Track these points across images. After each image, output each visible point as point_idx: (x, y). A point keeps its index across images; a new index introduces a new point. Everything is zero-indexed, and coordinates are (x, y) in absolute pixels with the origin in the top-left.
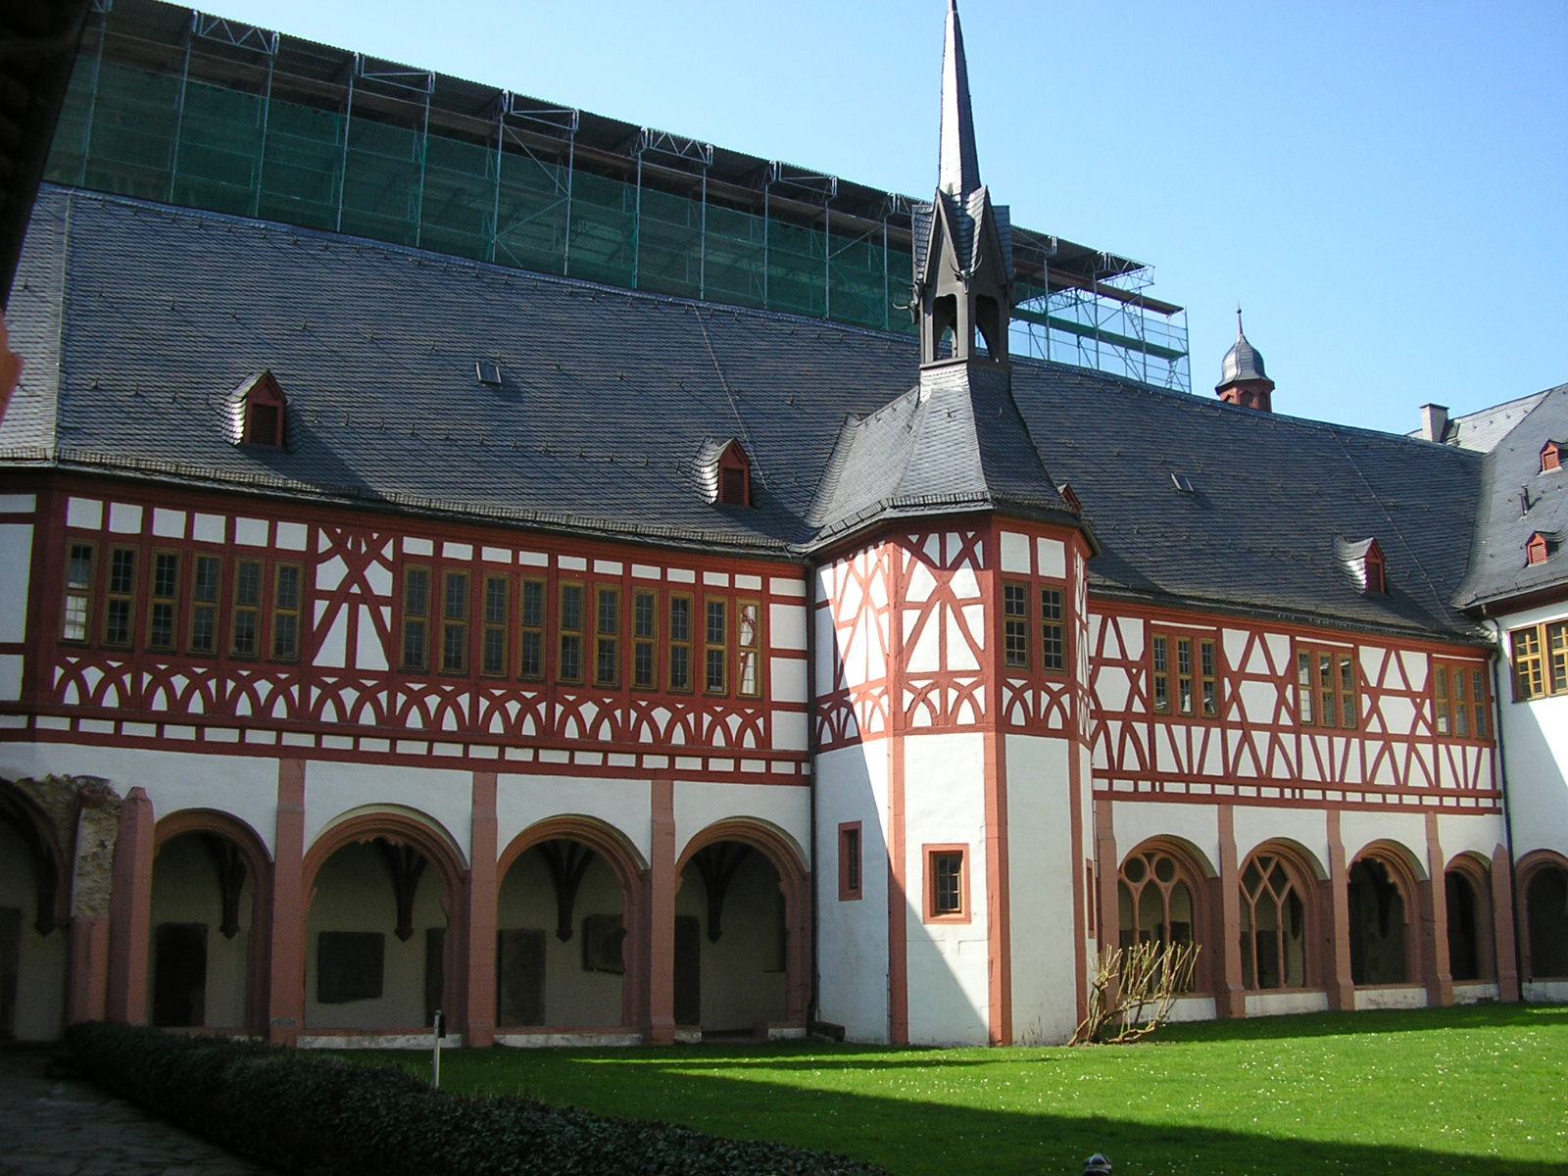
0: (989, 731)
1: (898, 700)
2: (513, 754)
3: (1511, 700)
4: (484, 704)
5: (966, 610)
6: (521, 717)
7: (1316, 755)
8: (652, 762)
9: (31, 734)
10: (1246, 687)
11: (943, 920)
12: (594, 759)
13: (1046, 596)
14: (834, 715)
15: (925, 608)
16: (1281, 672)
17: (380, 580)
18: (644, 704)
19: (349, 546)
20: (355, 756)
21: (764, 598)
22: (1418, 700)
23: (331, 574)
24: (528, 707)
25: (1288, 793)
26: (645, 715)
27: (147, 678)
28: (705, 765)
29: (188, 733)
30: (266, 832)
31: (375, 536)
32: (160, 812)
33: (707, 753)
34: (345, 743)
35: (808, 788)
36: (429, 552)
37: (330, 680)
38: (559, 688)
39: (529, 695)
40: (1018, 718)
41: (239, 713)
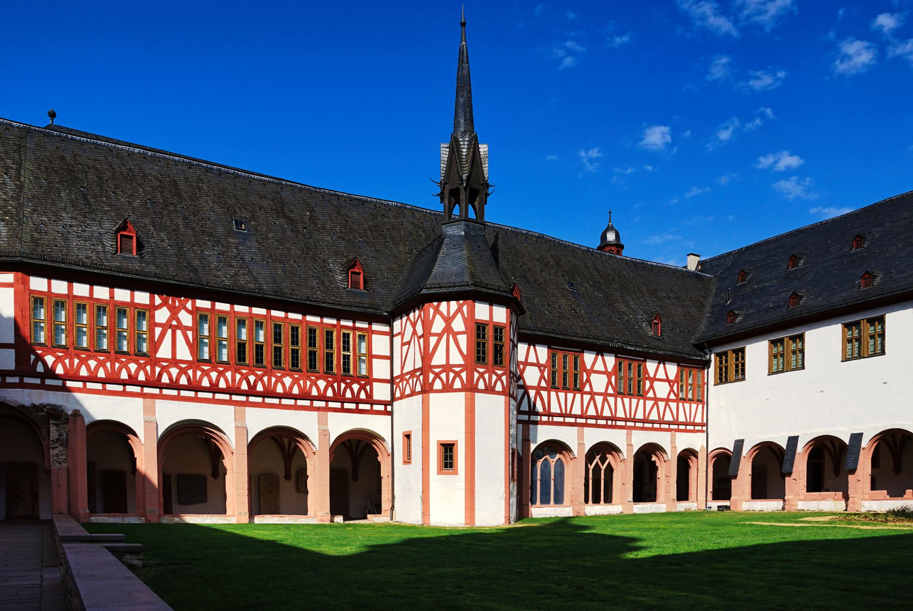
1: (426, 378)
2: (252, 399)
3: (713, 384)
5: (458, 337)
6: (256, 382)
7: (622, 407)
8: (317, 404)
9: (22, 385)
10: (593, 377)
12: (291, 402)
13: (496, 330)
14: (401, 384)
15: (440, 336)
16: (610, 369)
18: (313, 378)
22: (672, 384)
25: (610, 423)
28: (342, 405)
35: (390, 417)
36: (209, 307)
37: (165, 364)
39: (259, 373)
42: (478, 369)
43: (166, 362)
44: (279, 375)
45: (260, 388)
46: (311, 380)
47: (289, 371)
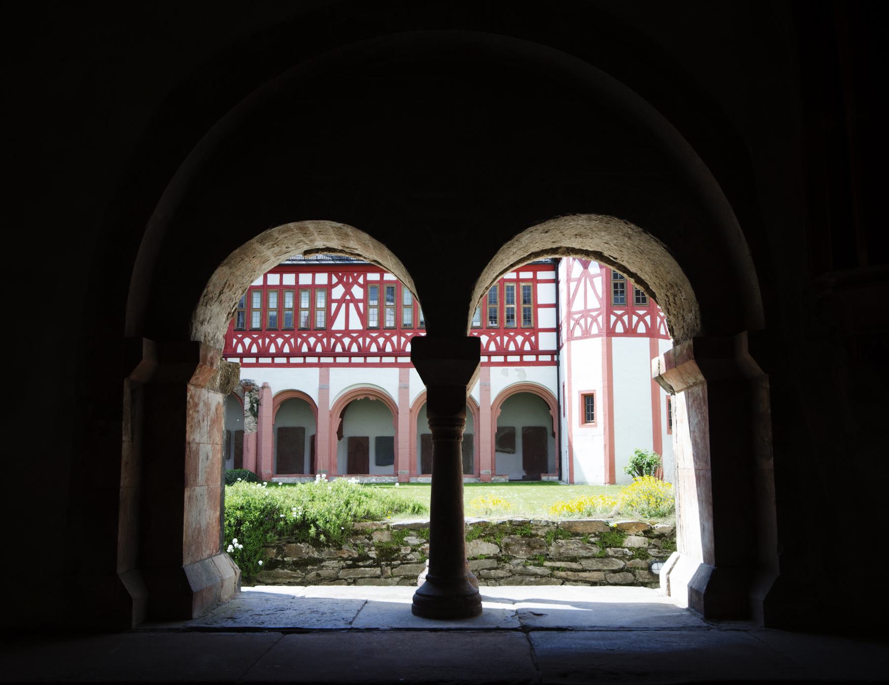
0: (603, 336)
11: (587, 426)
15: (579, 280)
17: (358, 292)
19: (345, 280)
20: (350, 365)
21: (535, 281)
23: (338, 292)
27: (267, 340)
28: (506, 359)
29: (283, 360)
31: (355, 274)
34: (346, 360)
35: (556, 367)
37: (339, 335)
42: (615, 312)
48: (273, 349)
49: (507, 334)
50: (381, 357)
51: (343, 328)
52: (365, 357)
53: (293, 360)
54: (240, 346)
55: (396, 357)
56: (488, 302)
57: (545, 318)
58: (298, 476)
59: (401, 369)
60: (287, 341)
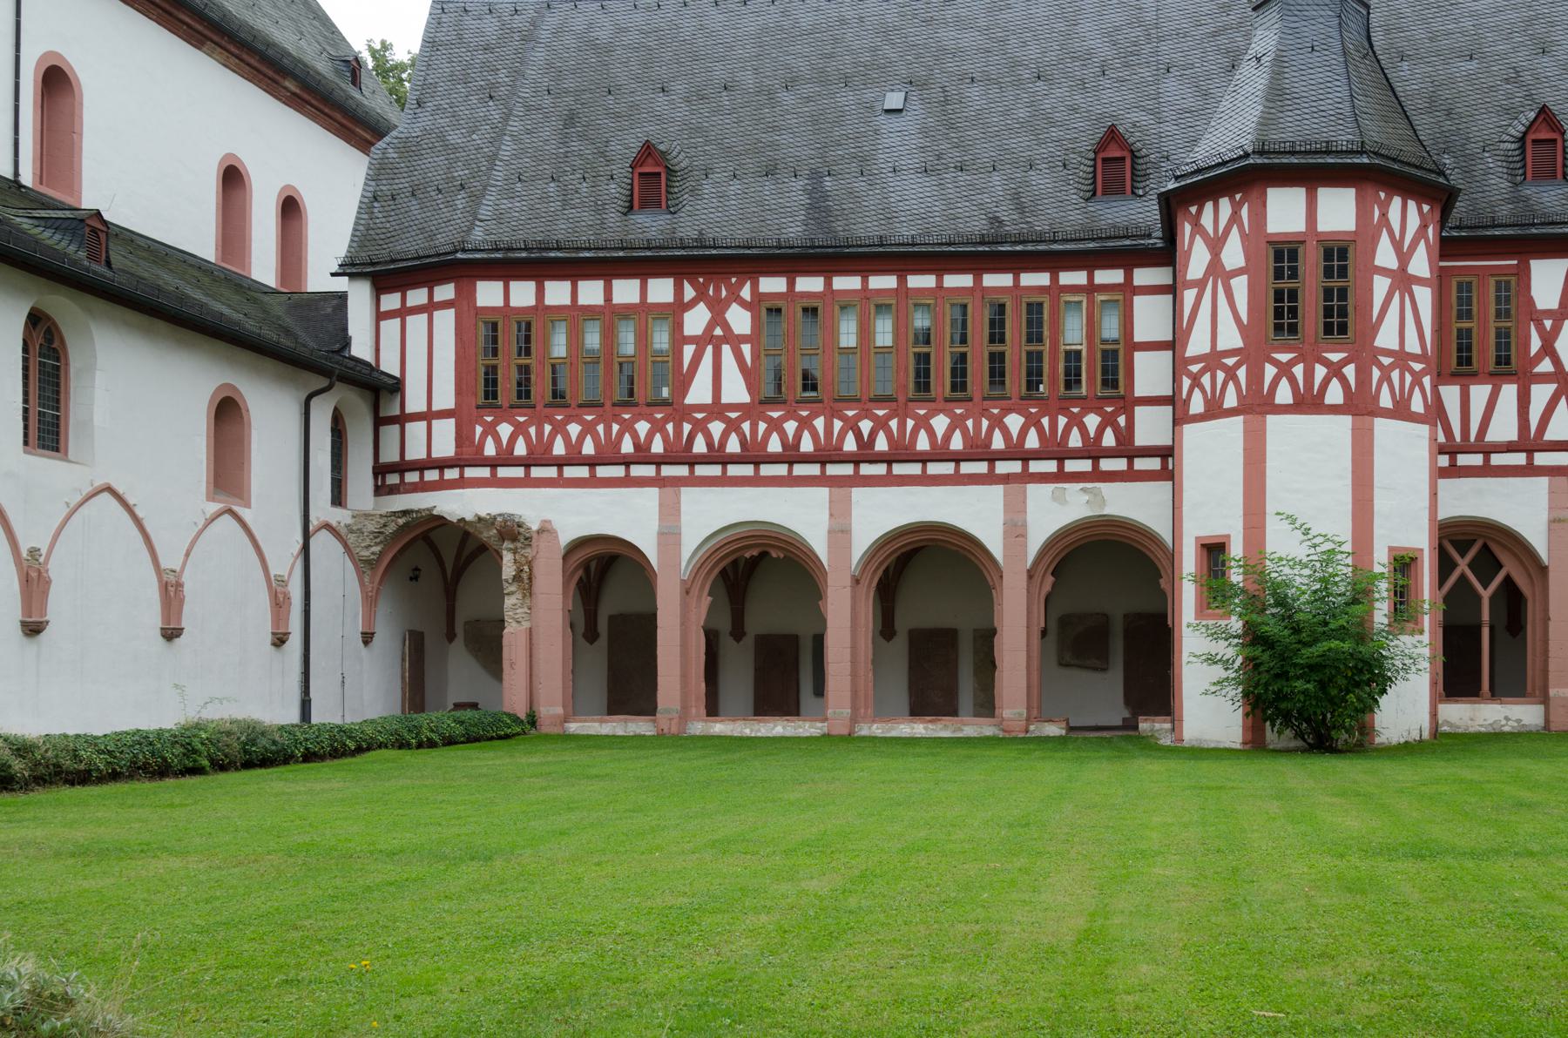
2: (866, 469)
4: (838, 424)
6: (873, 434)
8: (1002, 467)
9: (462, 483)
12: (947, 468)
17: (740, 320)
19: (711, 293)
20: (724, 481)
23: (696, 320)
24: (881, 424)
26: (998, 423)
27: (548, 428)
30: (650, 549)
31: (734, 280)
32: (566, 536)
33: (1061, 454)
34: (715, 470)
37: (699, 416)
38: (910, 404)
39: (881, 413)
40: (1386, 401)
41: (624, 450)
43: (700, 412)
44: (922, 412)
45: (881, 444)
46: (990, 417)
47: (943, 402)
48: (559, 449)
49: (1064, 411)
50: (791, 463)
51: (707, 399)
52: (757, 464)
53: (602, 472)
54: (490, 441)
55: (823, 464)
56: (1024, 338)
57: (1150, 374)
58: (621, 720)
59: (833, 489)
60: (588, 429)
